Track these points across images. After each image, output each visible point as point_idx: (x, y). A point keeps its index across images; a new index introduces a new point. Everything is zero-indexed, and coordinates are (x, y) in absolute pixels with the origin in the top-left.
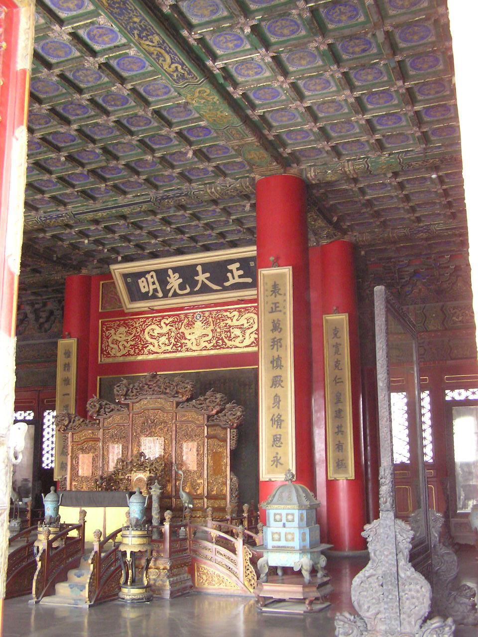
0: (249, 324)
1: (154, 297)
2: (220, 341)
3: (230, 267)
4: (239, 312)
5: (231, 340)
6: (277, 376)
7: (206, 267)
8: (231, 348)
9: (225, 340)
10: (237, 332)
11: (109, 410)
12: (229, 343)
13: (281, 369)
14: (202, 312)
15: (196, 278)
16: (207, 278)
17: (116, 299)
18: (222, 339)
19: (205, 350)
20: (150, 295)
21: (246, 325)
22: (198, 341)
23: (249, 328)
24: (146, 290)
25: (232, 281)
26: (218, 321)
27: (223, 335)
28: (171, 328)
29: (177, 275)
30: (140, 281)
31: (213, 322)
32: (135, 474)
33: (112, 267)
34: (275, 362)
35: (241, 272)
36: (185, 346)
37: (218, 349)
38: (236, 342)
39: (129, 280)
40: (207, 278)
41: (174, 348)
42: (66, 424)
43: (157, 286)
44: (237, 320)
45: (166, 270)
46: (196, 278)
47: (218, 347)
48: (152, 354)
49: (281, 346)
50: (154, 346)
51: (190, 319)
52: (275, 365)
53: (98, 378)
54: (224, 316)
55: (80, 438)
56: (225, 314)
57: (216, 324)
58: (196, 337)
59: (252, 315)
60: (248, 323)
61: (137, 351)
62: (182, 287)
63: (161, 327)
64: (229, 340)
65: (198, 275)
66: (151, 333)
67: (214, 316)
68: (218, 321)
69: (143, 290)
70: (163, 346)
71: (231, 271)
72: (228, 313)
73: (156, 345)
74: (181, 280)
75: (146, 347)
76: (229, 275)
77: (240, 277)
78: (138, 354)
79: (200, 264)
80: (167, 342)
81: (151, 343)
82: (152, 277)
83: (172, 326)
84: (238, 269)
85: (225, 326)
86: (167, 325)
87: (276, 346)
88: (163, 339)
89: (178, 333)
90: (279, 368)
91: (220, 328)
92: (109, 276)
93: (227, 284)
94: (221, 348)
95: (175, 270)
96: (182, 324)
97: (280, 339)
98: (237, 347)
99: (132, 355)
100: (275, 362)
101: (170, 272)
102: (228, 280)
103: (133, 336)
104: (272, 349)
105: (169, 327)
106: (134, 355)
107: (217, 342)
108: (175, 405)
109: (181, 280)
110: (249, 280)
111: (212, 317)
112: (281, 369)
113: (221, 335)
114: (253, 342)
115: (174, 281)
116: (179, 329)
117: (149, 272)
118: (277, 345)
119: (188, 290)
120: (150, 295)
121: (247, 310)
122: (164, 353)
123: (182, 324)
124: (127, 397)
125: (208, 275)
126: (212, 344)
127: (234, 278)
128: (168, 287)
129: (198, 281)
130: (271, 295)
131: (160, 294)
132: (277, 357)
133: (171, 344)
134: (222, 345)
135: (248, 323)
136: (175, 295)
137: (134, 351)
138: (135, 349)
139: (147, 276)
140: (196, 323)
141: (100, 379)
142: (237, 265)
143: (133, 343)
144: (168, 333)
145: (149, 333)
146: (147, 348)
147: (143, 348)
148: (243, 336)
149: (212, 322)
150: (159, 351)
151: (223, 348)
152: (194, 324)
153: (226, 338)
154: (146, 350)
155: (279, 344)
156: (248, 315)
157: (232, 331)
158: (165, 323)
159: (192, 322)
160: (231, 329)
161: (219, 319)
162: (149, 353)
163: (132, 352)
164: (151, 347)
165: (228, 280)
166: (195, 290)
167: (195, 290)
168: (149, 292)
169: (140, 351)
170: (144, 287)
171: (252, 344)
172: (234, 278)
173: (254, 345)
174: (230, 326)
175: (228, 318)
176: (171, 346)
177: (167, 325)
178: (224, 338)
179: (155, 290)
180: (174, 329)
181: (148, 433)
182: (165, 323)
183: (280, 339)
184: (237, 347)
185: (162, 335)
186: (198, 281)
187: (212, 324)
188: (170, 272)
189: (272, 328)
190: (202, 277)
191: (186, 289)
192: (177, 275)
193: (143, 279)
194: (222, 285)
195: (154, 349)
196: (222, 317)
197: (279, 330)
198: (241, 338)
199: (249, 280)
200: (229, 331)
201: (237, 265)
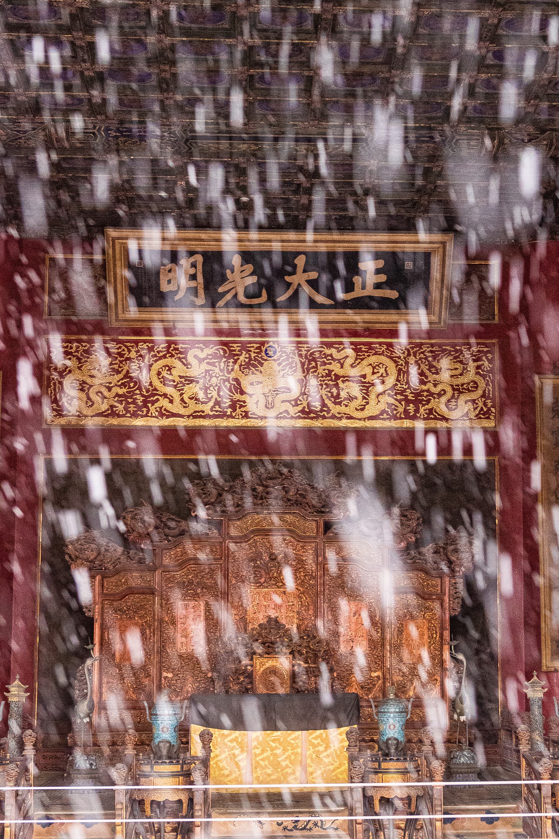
5: (340, 403)
8: (340, 419)
11: (176, 531)
12: (335, 409)
19: (284, 418)
22: (270, 399)
26: (313, 364)
32: (261, 660)
35: (383, 278)
36: (241, 406)
37: (312, 418)
41: (217, 408)
42: (92, 557)
44: (352, 366)
47: (312, 415)
48: (168, 417)
50: (171, 402)
51: (253, 355)
54: (326, 356)
55: (117, 586)
56: (328, 352)
58: (266, 391)
59: (383, 359)
60: (374, 373)
61: (132, 408)
64: (335, 403)
67: (304, 353)
68: (313, 364)
70: (191, 403)
72: (333, 351)
73: (177, 399)
75: (153, 403)
78: (135, 415)
79: (304, 253)
81: (165, 395)
83: (213, 364)
85: (329, 375)
86: (201, 361)
89: (228, 380)
94: (317, 418)
98: (350, 418)
99: (119, 416)
103: (121, 376)
105: (205, 366)
106: (123, 416)
108: (321, 530)
110: (393, 294)
114: (383, 412)
121: (371, 348)
122: (195, 417)
124: (218, 509)
126: (300, 408)
128: (221, 290)
133: (210, 399)
134: (322, 411)
135: (374, 373)
137: (126, 409)
138: (128, 403)
140: (266, 363)
143: (121, 391)
145: (159, 373)
146: (156, 405)
147: (145, 403)
148: (364, 398)
150: (182, 411)
151: (324, 417)
152: (262, 365)
153: (328, 398)
154: (152, 409)
156: (373, 359)
157: (341, 385)
158: (195, 357)
159: (255, 360)
160: (339, 382)
162: (162, 415)
163: (120, 408)
164: (164, 403)
169: (139, 408)
173: (385, 416)
174: (337, 377)
176: (211, 404)
177: (201, 361)
180: (217, 370)
181: (262, 580)
182: (195, 357)
184: (350, 418)
195: (176, 408)
198: (360, 401)
199: (393, 294)
200: (337, 386)
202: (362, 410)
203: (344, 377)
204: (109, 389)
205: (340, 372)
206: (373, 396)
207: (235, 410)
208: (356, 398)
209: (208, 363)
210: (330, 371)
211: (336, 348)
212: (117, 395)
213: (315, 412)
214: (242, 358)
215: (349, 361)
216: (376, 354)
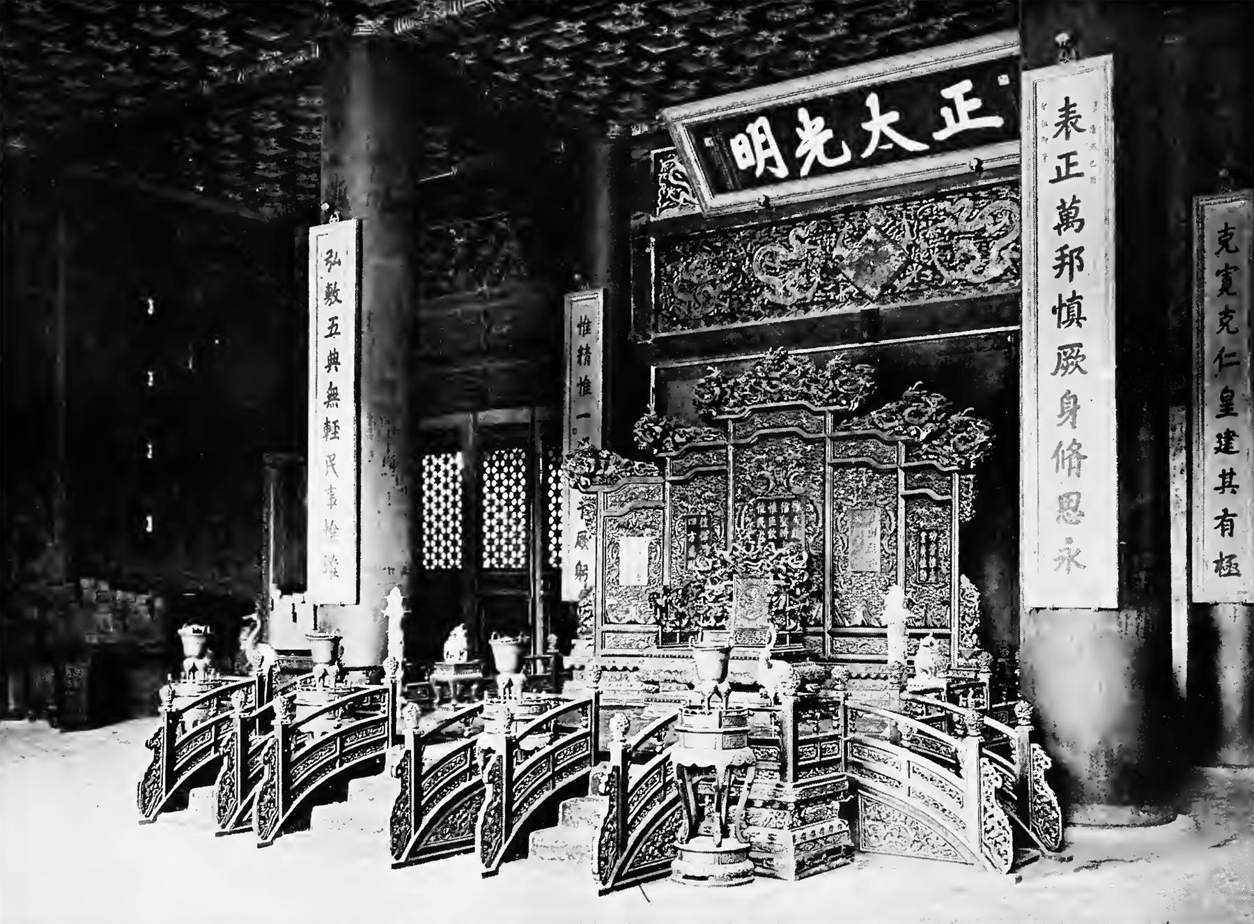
0: (998, 227)
1: (769, 179)
2: (928, 272)
3: (947, 93)
4: (975, 198)
5: (954, 268)
6: (1071, 346)
7: (890, 94)
9: (939, 267)
10: (969, 246)
13: (1080, 325)
14: (884, 204)
15: (866, 126)
16: (892, 125)
17: (684, 189)
18: (933, 267)
20: (759, 172)
21: (991, 229)
23: (998, 237)
24: (750, 162)
25: (952, 129)
26: (924, 224)
27: (935, 257)
28: (812, 247)
29: (820, 121)
30: (734, 143)
31: (912, 226)
33: (670, 113)
34: (1065, 310)
35: (976, 103)
38: (968, 273)
39: (708, 142)
40: (892, 125)
41: (820, 293)
43: (774, 151)
44: (968, 220)
45: (793, 108)
46: (866, 126)
49: (1081, 268)
50: (773, 292)
52: (1064, 318)
53: (653, 369)
57: (918, 231)
62: (832, 149)
63: (789, 248)
64: (949, 269)
65: (868, 117)
66: (767, 261)
68: (924, 224)
69: (743, 164)
71: (951, 103)
74: (829, 134)
75: (756, 295)
76: (946, 112)
77: (973, 115)
80: (803, 282)
82: (761, 130)
83: (815, 243)
84: (967, 96)
86: (802, 241)
87: (1067, 268)
88: (795, 275)
90: (1074, 324)
91: (927, 240)
92: (663, 136)
93: (940, 136)
95: (816, 107)
96: (837, 237)
97: (1081, 249)
100: (1065, 310)
101: (803, 114)
102: (942, 124)
104: (1058, 276)
107: (919, 275)
109: (829, 134)
110: (996, 122)
111: (908, 217)
112: (1080, 325)
113: (929, 258)
115: (814, 136)
116: (831, 249)
117: (752, 117)
118: (1071, 264)
119: (847, 156)
120: (759, 172)
123: (837, 237)
125: (894, 116)
126: (908, 280)
127: (957, 120)
128: (799, 153)
129: (870, 133)
130: (1055, 136)
131: (781, 171)
132: (1070, 296)
134: (933, 279)
135: (995, 224)
136: (817, 170)
139: (748, 130)
141: (657, 371)
142: (967, 85)
144: (806, 259)
148: (983, 257)
149: (907, 228)
155: (1076, 263)
158: (798, 237)
161: (926, 219)
165: (942, 124)
166: (865, 155)
167: (865, 155)
168: (754, 167)
170: (744, 156)
171: (1005, 273)
172: (957, 120)
174: (952, 235)
175: (947, 214)
178: (937, 263)
179: (771, 162)
182: (798, 237)
183: (1081, 249)
185: (793, 264)
186: (870, 133)
187: (908, 233)
188: (803, 114)
189: (1057, 220)
190: (880, 123)
191: (840, 153)
192: (820, 121)
193: (741, 137)
194: (927, 139)
196: (932, 215)
197: (1077, 225)
199: (996, 122)
200: (950, 247)
201: (967, 85)
202: (981, 272)
203: (960, 233)
204: (714, 286)
205: (953, 227)
206: (994, 252)
207: (838, 293)
208: (974, 258)
209: (810, 243)
210: (943, 229)
211: (950, 200)
212: (723, 292)
213: (927, 283)
214: (845, 230)
215: (964, 215)
216: (998, 199)
